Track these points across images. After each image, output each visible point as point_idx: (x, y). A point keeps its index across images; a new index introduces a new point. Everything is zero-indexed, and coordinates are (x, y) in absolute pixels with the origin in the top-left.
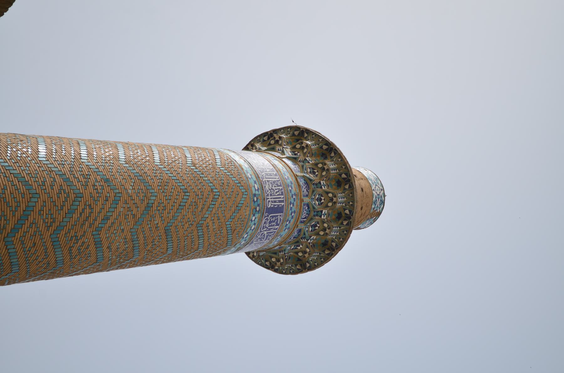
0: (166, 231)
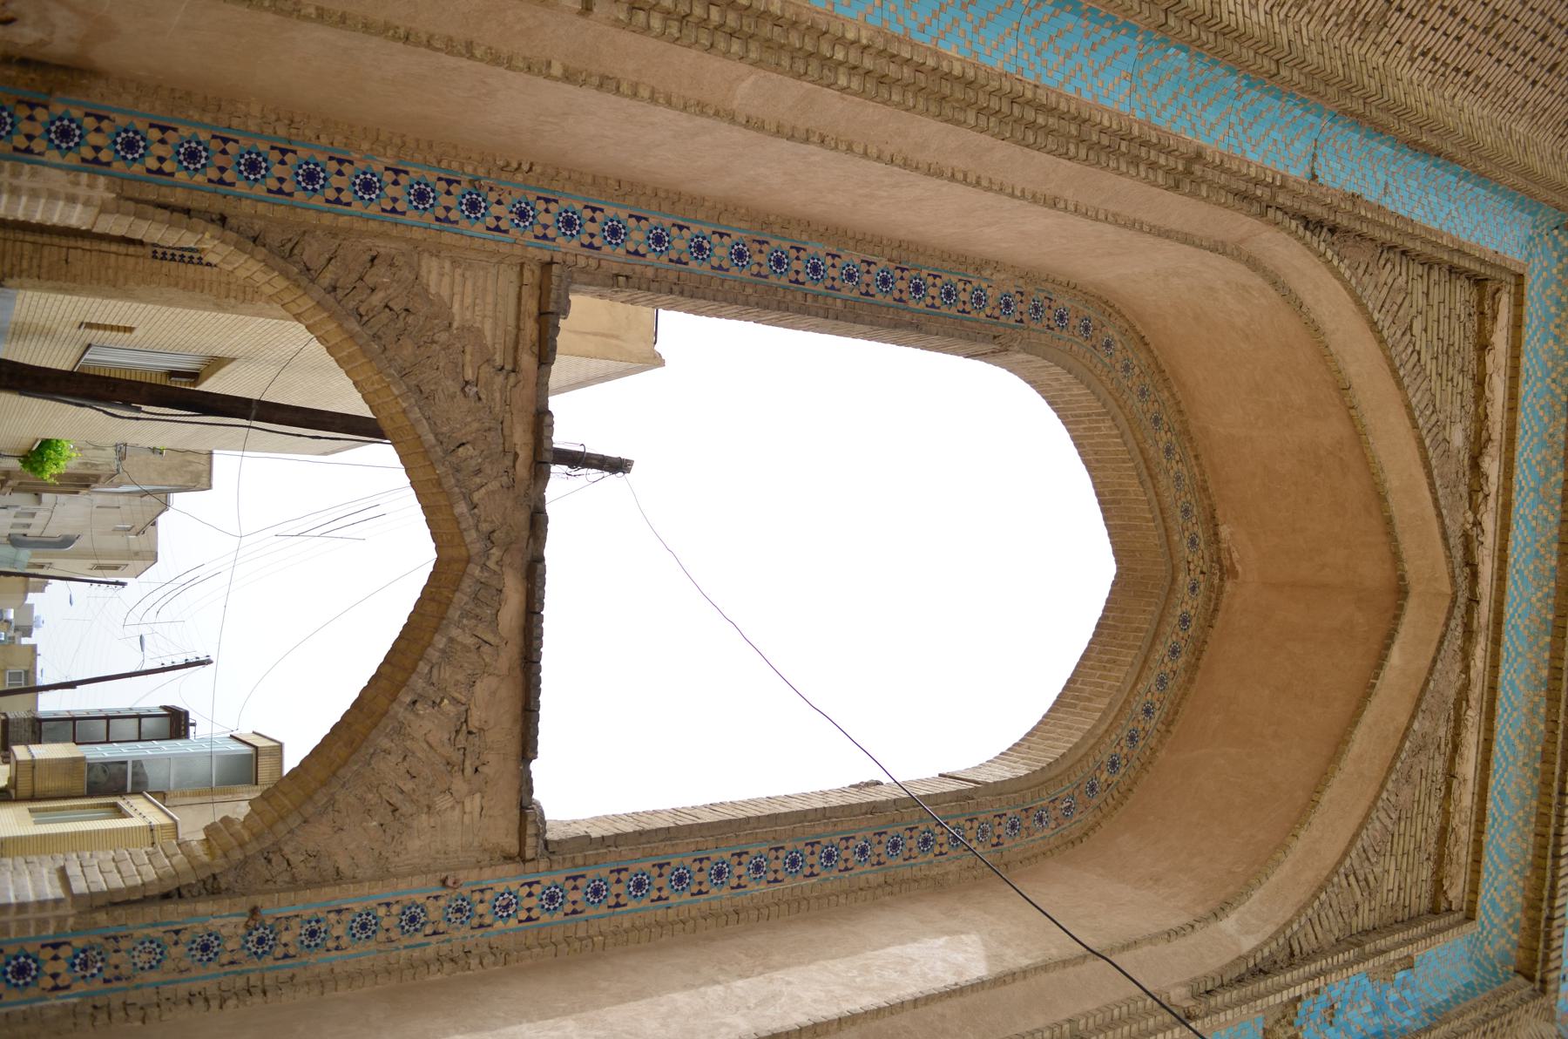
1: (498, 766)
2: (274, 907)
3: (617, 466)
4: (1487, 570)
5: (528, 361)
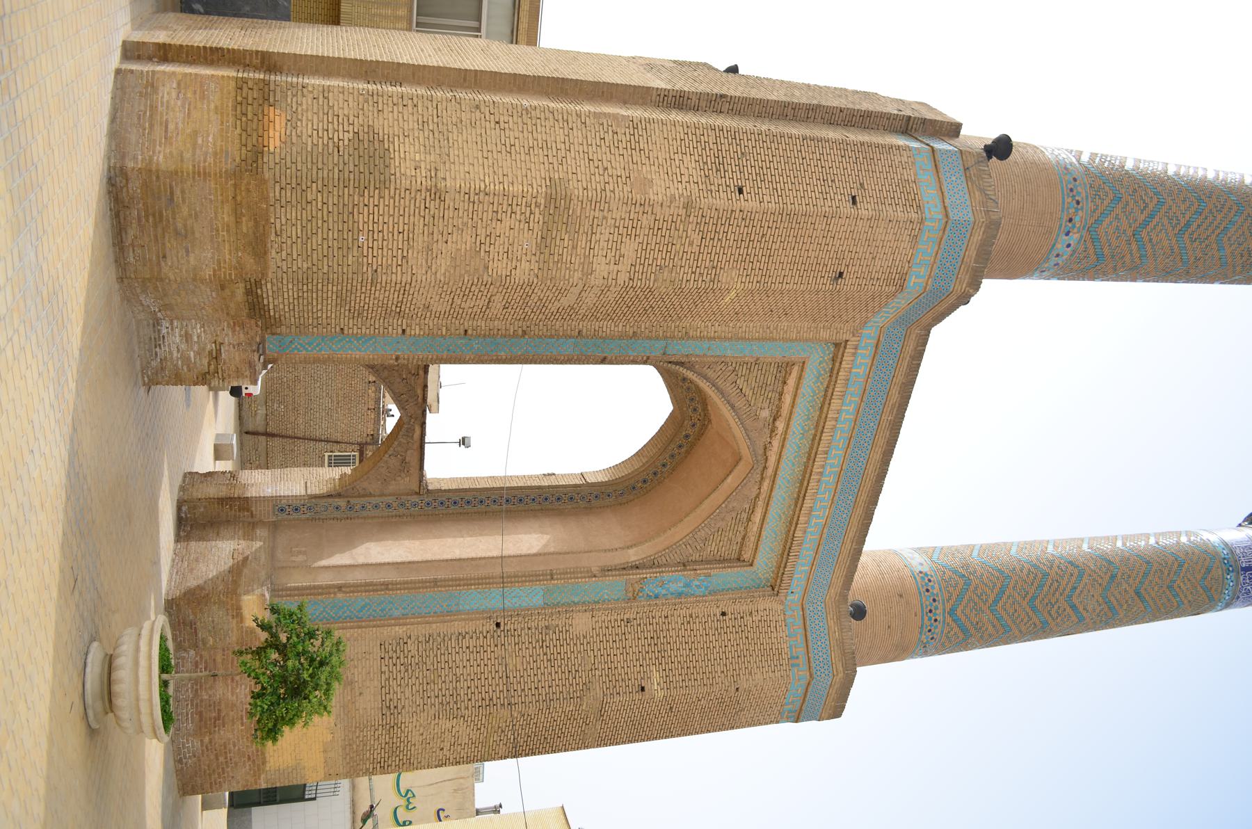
0: (1137, 593)
1: (414, 471)
2: (353, 501)
5: (421, 372)
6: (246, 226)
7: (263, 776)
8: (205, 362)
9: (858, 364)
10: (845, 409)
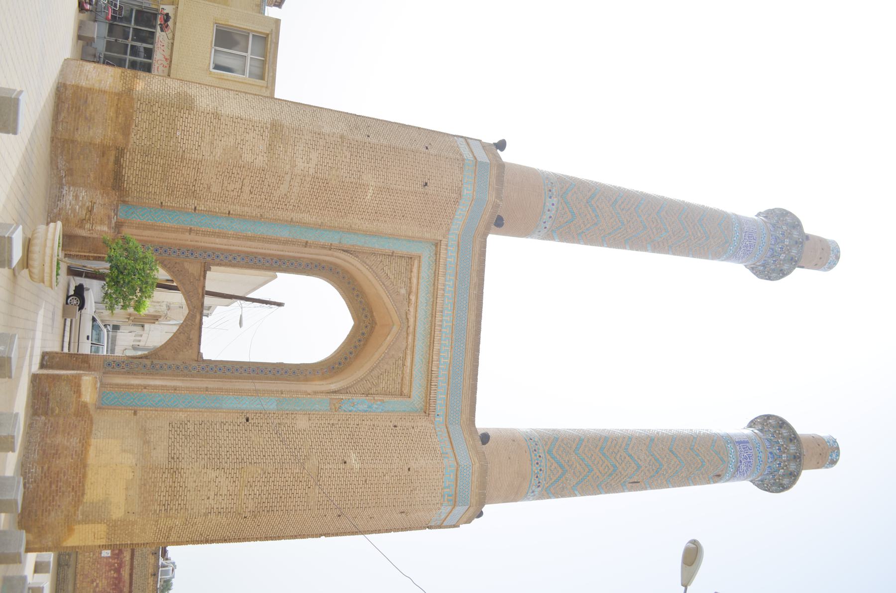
2: (155, 362)
3: (280, 305)
4: (412, 320)
6: (121, 119)
7: (81, 508)
8: (84, 213)
9: (449, 255)
10: (447, 283)
